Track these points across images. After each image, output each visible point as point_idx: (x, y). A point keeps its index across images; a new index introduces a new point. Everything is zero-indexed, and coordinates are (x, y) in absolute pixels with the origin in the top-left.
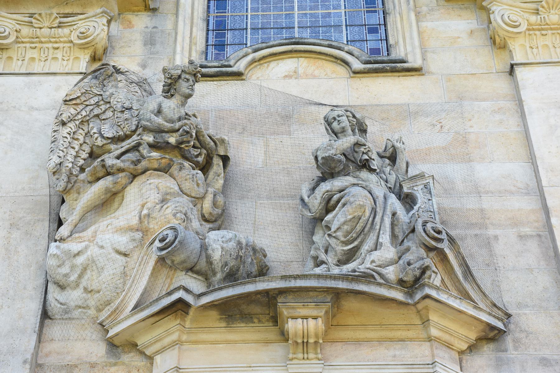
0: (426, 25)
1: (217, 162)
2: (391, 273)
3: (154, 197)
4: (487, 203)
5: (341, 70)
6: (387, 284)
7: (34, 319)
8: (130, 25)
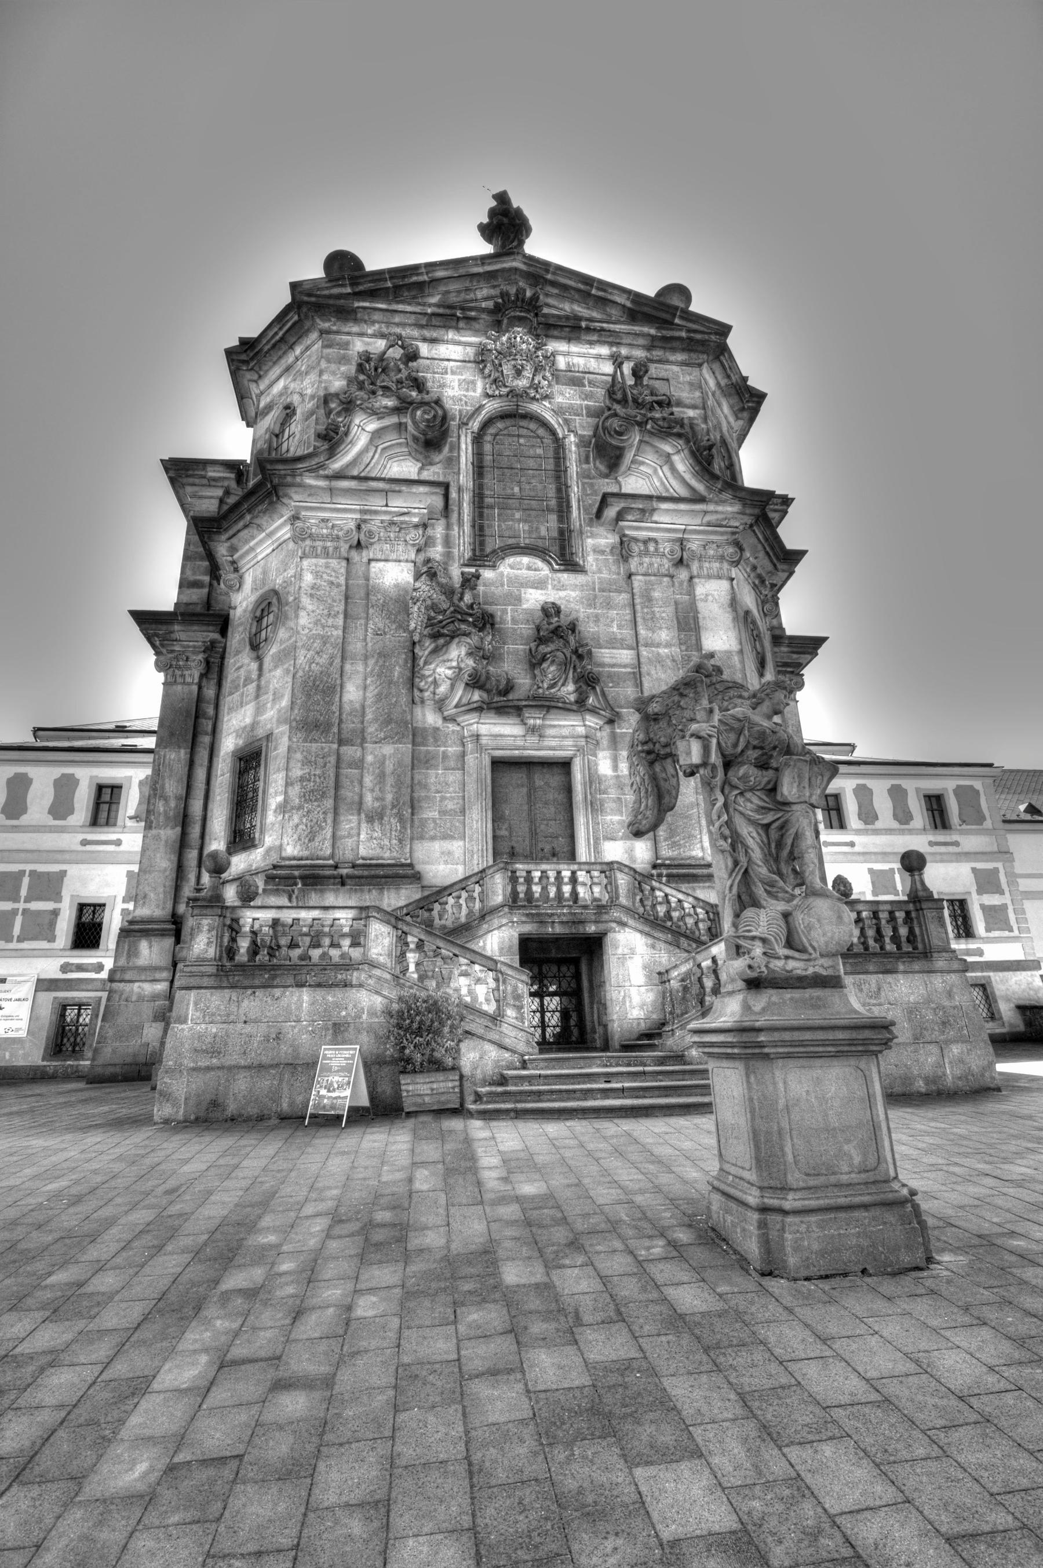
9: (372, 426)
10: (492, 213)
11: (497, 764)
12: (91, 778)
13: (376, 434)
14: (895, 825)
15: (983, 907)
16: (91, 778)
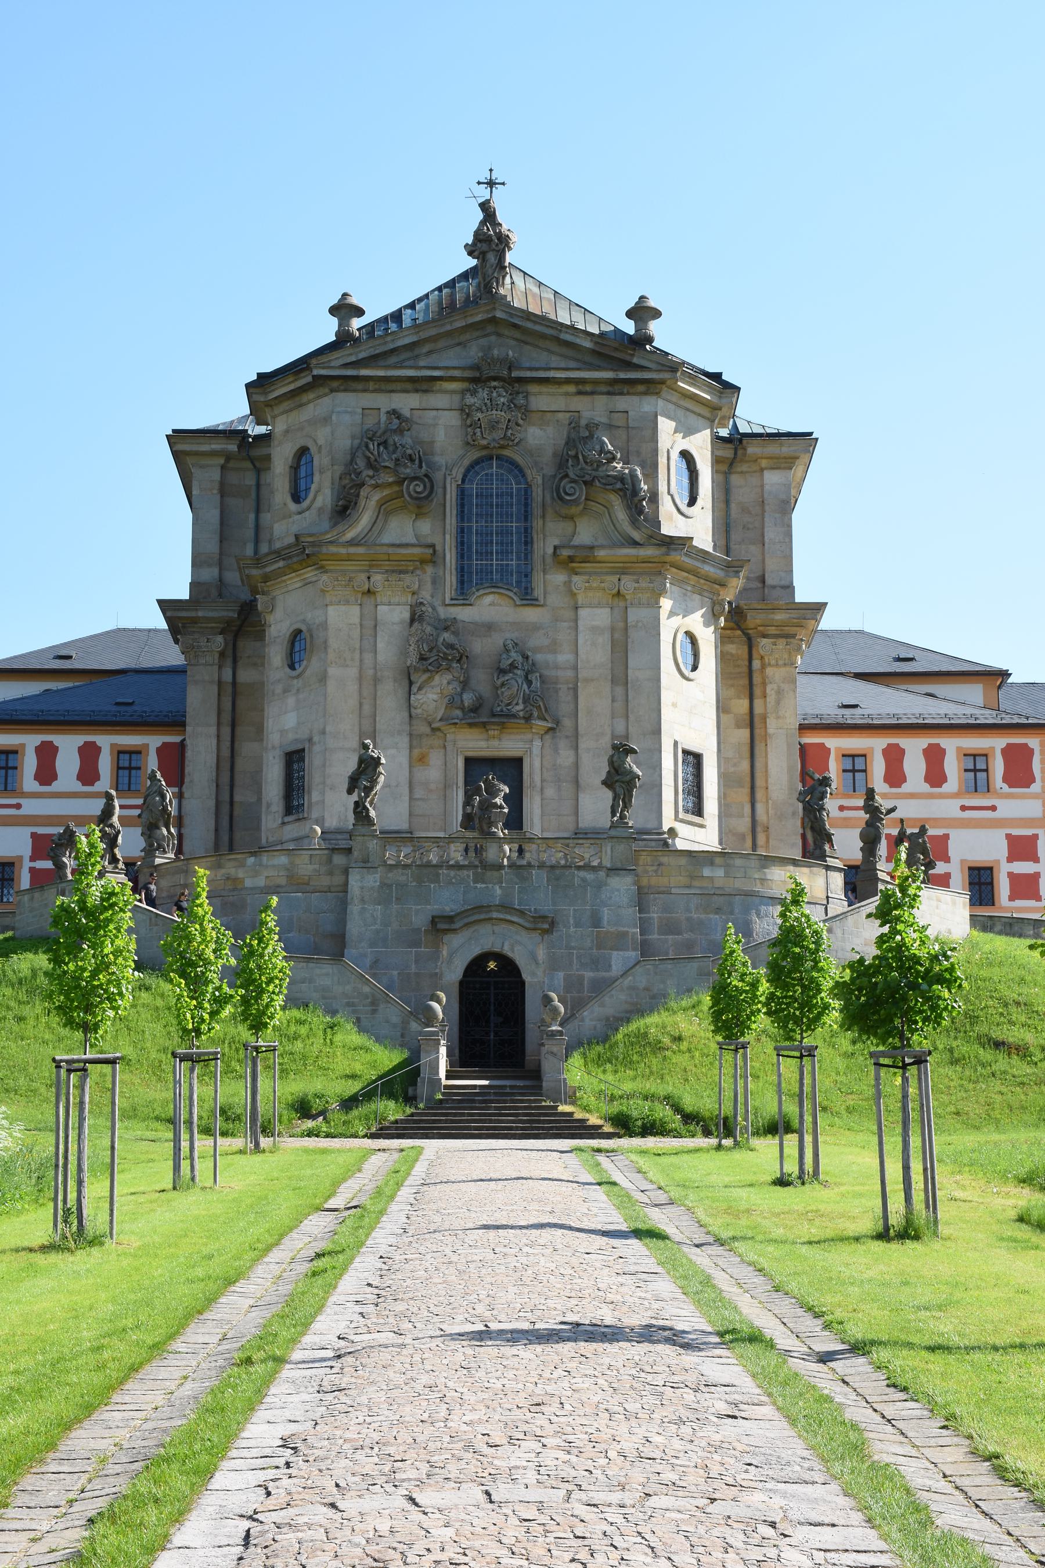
0: (547, 576)
1: (464, 658)
2: (521, 714)
3: (445, 682)
4: (560, 673)
5: (511, 601)
6: (520, 718)
7: (407, 719)
8: (425, 572)
9: (376, 496)
10: (477, 234)
11: (469, 761)
12: (113, 746)
13: (381, 504)
14: (926, 788)
15: (1011, 875)
16: (113, 746)
